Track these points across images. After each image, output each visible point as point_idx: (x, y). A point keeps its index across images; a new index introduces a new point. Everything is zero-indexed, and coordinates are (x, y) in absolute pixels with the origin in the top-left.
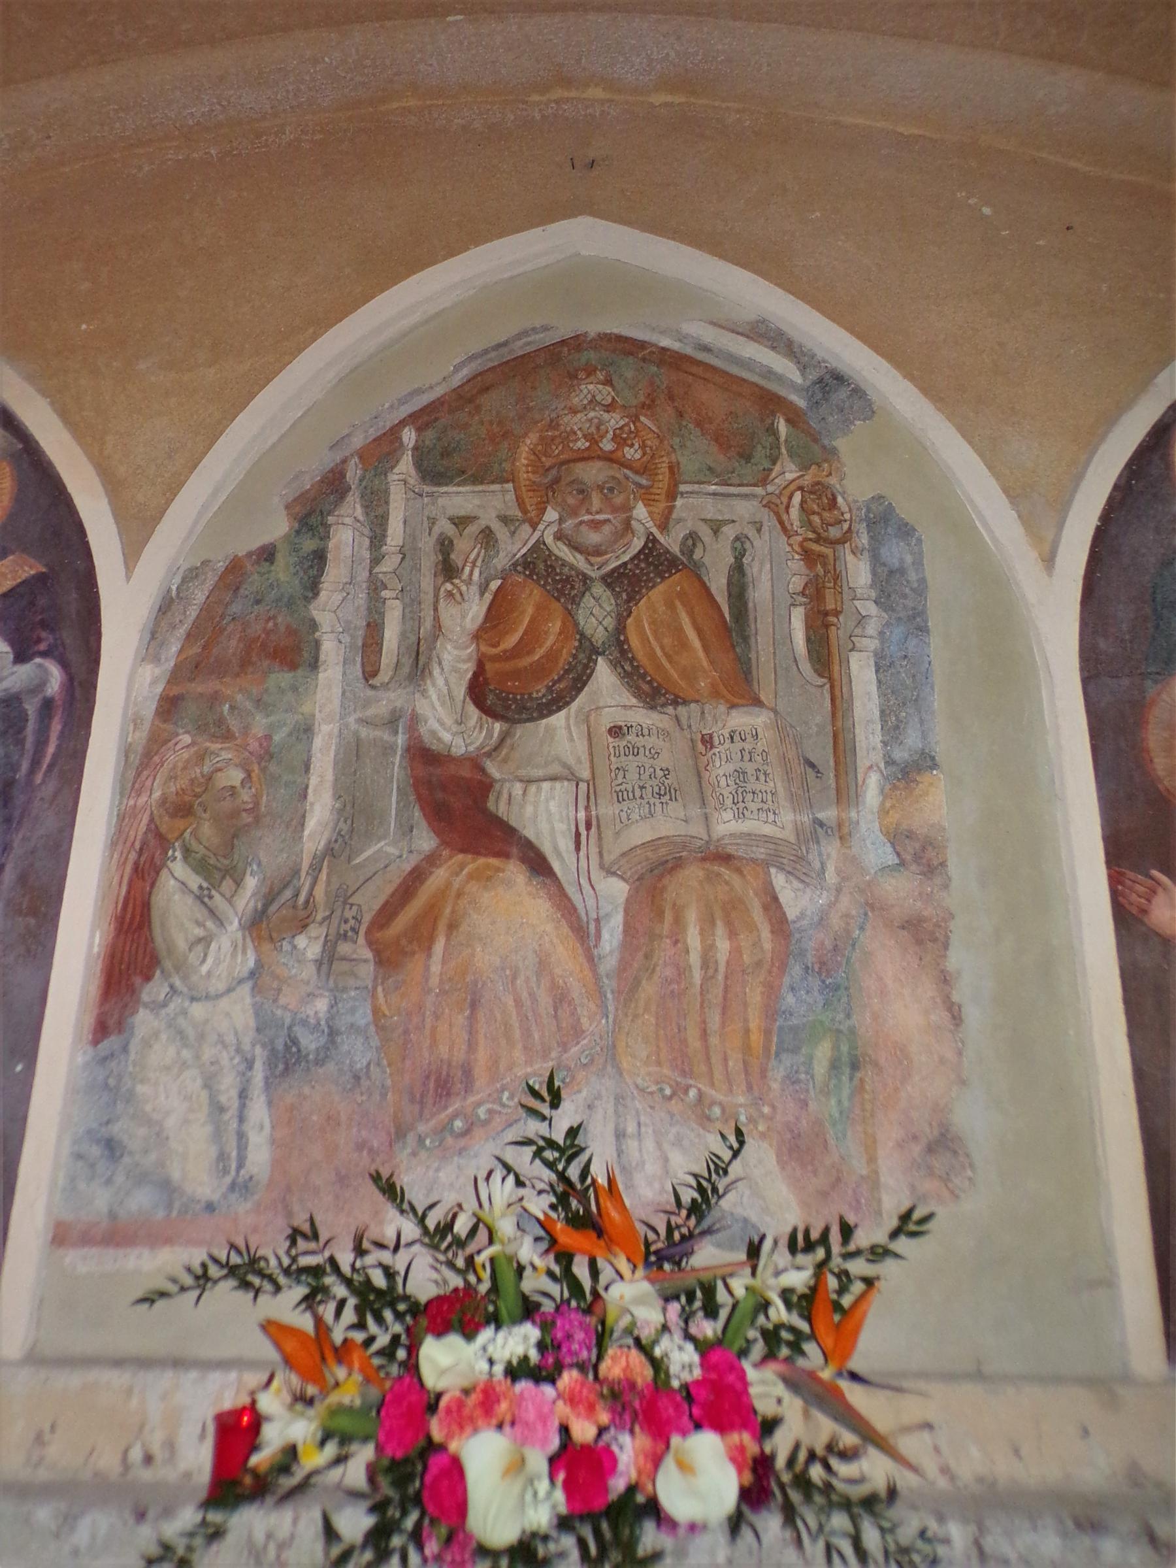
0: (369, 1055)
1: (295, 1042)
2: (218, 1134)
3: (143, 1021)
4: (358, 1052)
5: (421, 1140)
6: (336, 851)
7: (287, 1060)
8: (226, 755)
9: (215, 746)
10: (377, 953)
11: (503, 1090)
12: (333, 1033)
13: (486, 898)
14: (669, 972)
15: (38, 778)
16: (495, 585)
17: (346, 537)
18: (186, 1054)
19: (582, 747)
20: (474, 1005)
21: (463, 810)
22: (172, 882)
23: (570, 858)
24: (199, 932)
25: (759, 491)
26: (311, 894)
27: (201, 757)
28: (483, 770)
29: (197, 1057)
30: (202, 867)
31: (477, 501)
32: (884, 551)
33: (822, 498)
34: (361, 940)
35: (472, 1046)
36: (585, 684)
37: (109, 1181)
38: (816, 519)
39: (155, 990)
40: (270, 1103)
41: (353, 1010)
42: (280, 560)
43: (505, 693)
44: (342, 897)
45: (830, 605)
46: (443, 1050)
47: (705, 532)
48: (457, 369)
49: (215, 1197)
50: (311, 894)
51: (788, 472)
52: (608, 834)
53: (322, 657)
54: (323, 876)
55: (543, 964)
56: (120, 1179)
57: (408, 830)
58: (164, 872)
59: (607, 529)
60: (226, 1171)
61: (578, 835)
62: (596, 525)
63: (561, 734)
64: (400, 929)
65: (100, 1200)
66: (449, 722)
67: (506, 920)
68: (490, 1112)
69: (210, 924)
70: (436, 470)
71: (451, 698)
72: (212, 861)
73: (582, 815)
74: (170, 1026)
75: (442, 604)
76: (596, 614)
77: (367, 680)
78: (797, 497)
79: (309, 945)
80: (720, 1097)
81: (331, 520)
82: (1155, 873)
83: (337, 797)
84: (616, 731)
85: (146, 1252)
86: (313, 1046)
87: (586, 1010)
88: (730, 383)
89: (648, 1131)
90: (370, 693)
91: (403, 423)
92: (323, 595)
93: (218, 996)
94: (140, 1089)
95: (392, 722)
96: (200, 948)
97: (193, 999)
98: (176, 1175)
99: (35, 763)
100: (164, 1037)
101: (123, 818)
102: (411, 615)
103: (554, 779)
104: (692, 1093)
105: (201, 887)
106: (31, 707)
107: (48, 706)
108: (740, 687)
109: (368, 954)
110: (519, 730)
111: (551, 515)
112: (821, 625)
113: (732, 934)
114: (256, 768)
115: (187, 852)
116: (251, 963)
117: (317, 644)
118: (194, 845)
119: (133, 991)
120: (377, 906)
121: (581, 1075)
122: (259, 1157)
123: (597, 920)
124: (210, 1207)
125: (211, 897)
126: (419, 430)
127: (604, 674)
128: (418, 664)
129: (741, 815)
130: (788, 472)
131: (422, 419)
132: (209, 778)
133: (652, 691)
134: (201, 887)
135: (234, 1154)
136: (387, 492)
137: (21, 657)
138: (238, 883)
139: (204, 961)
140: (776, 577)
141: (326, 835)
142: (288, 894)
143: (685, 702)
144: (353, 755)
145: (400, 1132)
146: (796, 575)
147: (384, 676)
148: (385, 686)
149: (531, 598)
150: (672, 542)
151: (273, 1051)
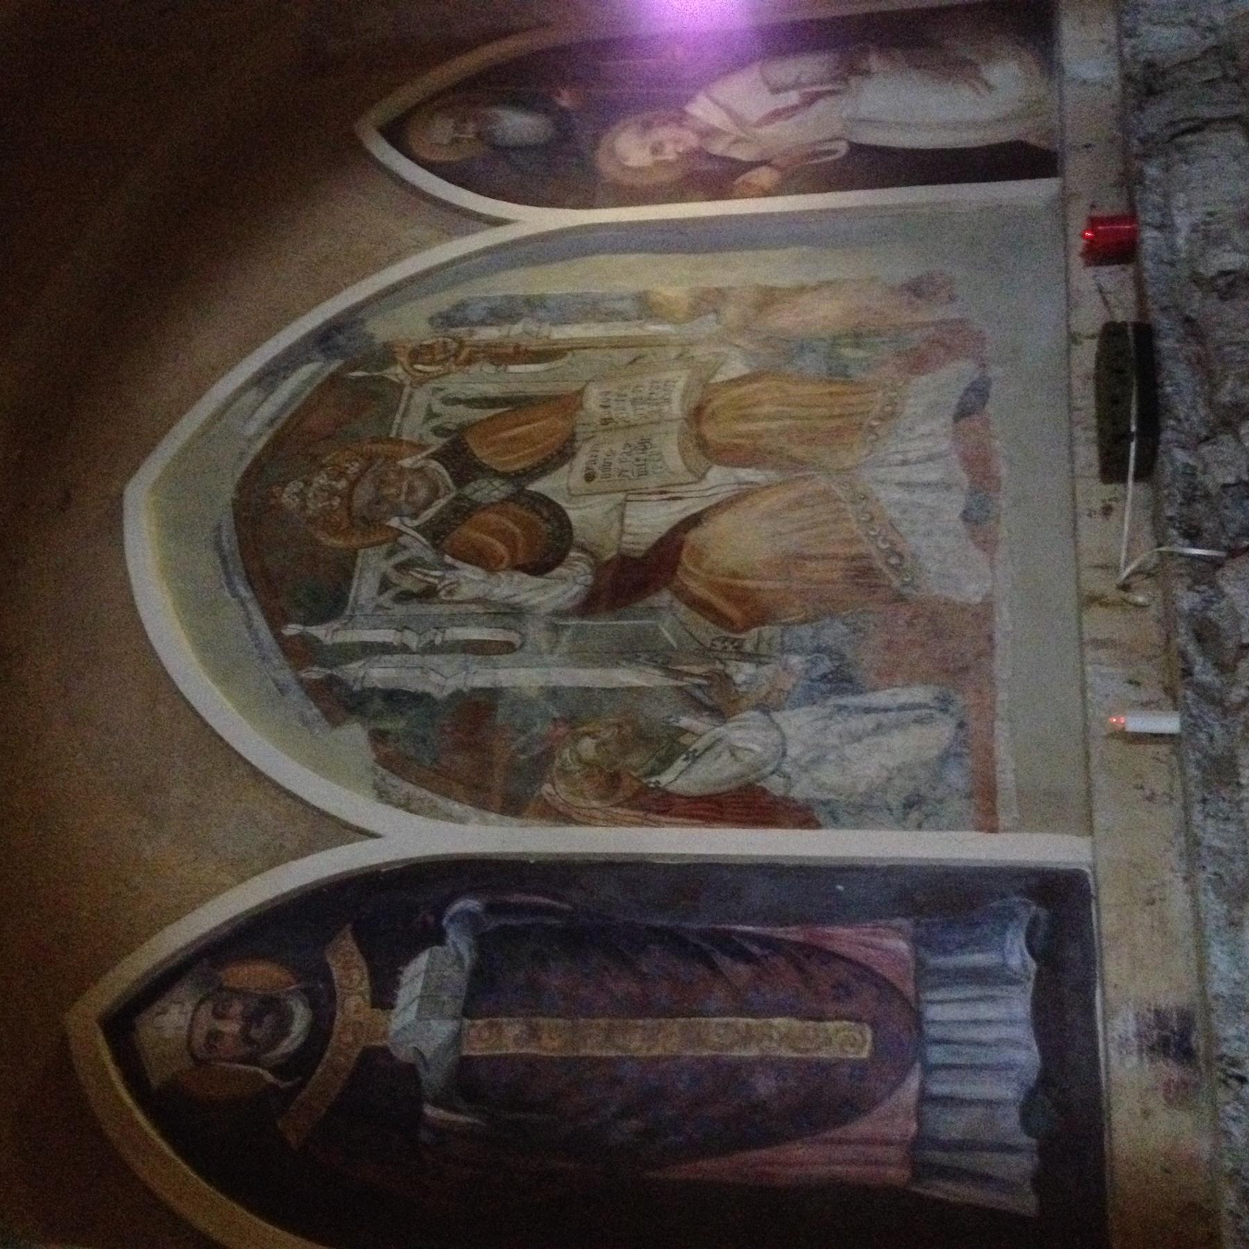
0: (837, 623)
1: (824, 676)
2: (900, 726)
3: (801, 790)
4: (834, 632)
5: (905, 585)
6: (665, 662)
7: (840, 681)
8: (566, 753)
9: (557, 762)
10: (755, 624)
11: (867, 534)
12: (819, 649)
13: (713, 557)
14: (783, 439)
15: (566, 906)
16: (448, 559)
18: (831, 757)
19: (599, 498)
20: (804, 558)
22: (678, 782)
23: (689, 502)
24: (726, 756)
25: (407, 390)
26: (700, 676)
27: (564, 773)
28: (609, 562)
29: (835, 747)
30: (666, 762)
31: (368, 575)
32: (475, 319)
34: (743, 636)
35: (835, 557)
36: (546, 498)
37: (941, 801)
38: (438, 358)
39: (775, 785)
40: (874, 690)
41: (800, 638)
42: (387, 725)
44: (705, 652)
45: (511, 350)
46: (835, 575)
47: (435, 423)
48: (235, 594)
49: (952, 723)
50: (700, 676)
51: (396, 372)
52: (673, 479)
53: (488, 685)
54: (685, 668)
55: (771, 515)
56: (939, 793)
57: (653, 611)
58: (670, 788)
59: (417, 483)
60: (931, 716)
61: (669, 499)
62: (412, 490)
63: (587, 514)
65: (956, 805)
66: (564, 587)
68: (884, 541)
69: (718, 749)
71: (544, 586)
72: (663, 753)
73: (654, 497)
74: (806, 771)
75: (456, 598)
76: (488, 490)
77: (515, 650)
78: (419, 367)
79: (743, 672)
80: (878, 407)
81: (357, 688)
82: (736, 183)
83: (617, 665)
84: (589, 477)
85: (999, 768)
86: (828, 663)
87: (808, 488)
88: (308, 408)
89: (900, 447)
90: (528, 648)
91: (278, 636)
92: (429, 689)
93: (783, 736)
94: (862, 788)
95: (556, 629)
96: (739, 754)
97: (784, 754)
98: (936, 752)
99: (550, 911)
100: (816, 774)
101: (614, 822)
102: (464, 620)
103: (622, 517)
104: (875, 423)
105: (686, 759)
106: (492, 923)
107: (490, 909)
108: (568, 403)
109: (754, 631)
110: (578, 537)
111: (394, 522)
113: (758, 404)
114: (581, 730)
115: (653, 772)
116: (756, 713)
117: (474, 690)
118: (647, 768)
119: (775, 801)
120: (713, 628)
121: (860, 489)
122: (920, 694)
123: (739, 484)
124: (961, 725)
125: (695, 750)
126: (288, 620)
129: (668, 401)
130: (396, 372)
131: (276, 619)
132: (587, 764)
133: (563, 454)
134: (686, 759)
135: (917, 712)
136: (340, 645)
137: (438, 937)
138: (684, 731)
139: (751, 750)
141: (649, 670)
142: (698, 693)
143: (574, 435)
144: (581, 657)
145: (900, 598)
147: (514, 637)
148: (523, 636)
149: (468, 533)
150: (437, 443)
151: (831, 691)
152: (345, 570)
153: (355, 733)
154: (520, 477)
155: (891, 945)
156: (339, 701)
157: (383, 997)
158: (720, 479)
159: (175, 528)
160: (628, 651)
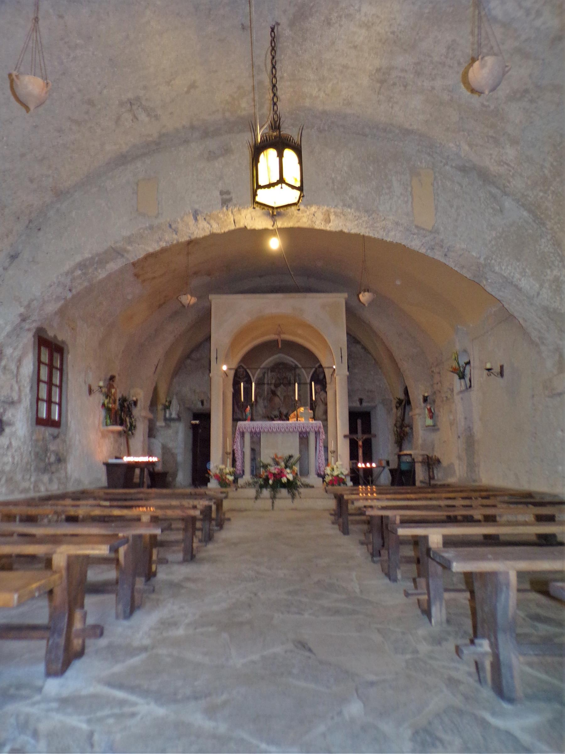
17: (266, 376)
21: (274, 393)
33: (295, 373)
43: (277, 386)
63: (279, 389)
64: (271, 400)
67: (277, 400)
70: (271, 371)
140: (292, 378)
153: (261, 375)
158: (282, 398)
160: (268, 394)
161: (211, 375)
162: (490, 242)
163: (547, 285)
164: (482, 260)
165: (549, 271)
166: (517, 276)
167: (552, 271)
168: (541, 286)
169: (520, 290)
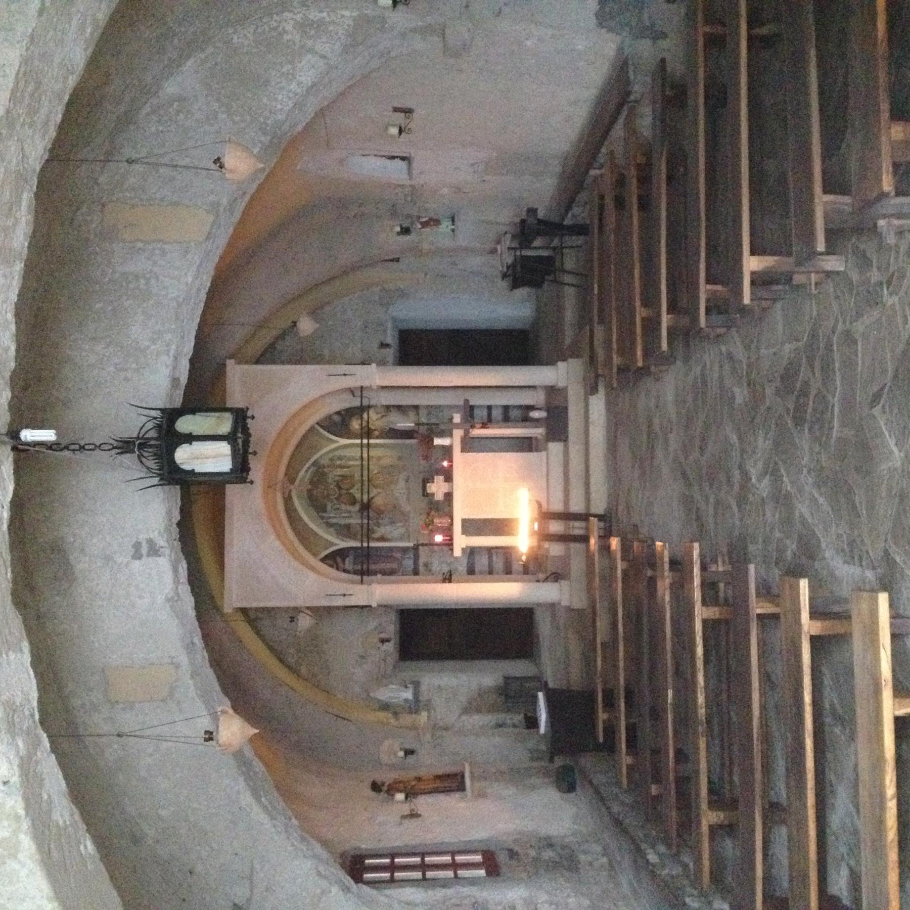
17: (334, 521)
51: (325, 470)
76: (344, 492)
112: (344, 467)
127: (351, 491)
128: (349, 512)
130: (325, 470)
131: (318, 513)
146: (339, 470)
152: (325, 506)
153: (332, 530)
154: (347, 490)
155: (399, 555)
156: (329, 525)
157: (344, 564)
159: (299, 497)
161: (374, 605)
162: (234, 123)
163: (309, 43)
164: (266, 139)
165: (287, 37)
166: (293, 86)
167: (285, 31)
168: (311, 51)
169: (314, 85)
